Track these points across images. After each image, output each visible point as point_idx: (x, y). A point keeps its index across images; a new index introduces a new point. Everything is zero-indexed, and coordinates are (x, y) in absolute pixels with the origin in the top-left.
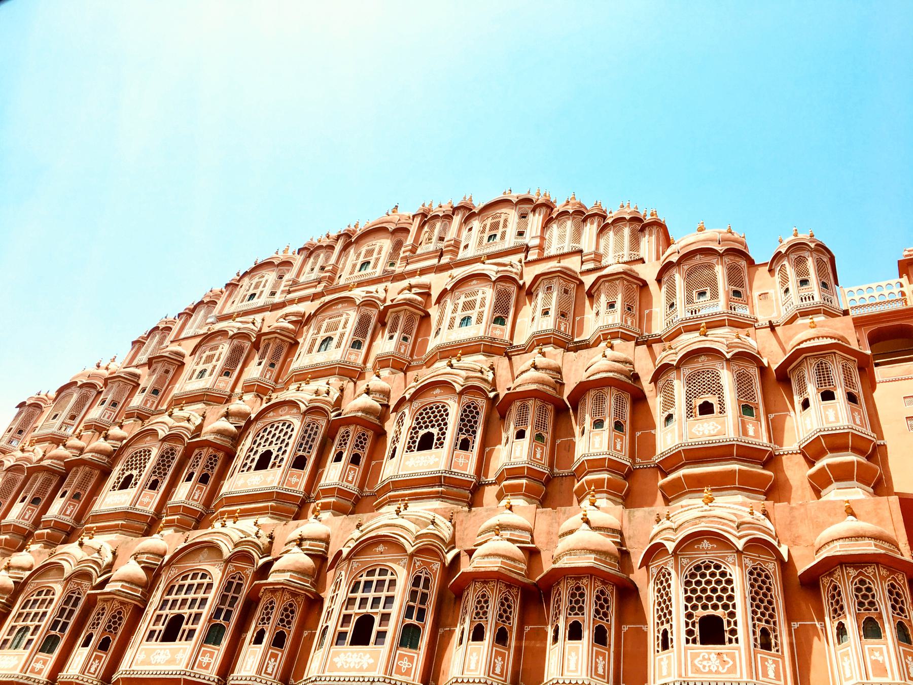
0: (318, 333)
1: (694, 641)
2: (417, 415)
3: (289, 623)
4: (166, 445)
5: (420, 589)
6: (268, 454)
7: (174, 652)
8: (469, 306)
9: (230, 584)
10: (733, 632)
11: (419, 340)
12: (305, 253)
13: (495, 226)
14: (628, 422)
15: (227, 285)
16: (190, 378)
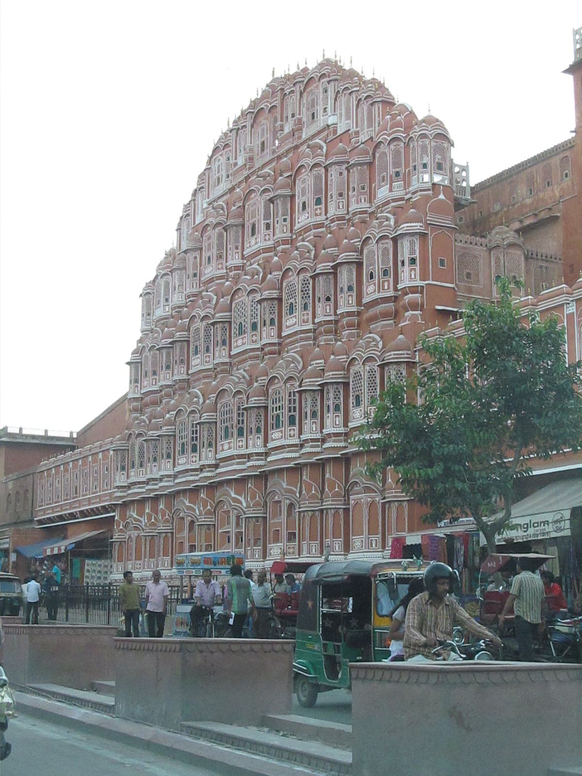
1: (354, 407)
3: (260, 421)
4: (204, 323)
5: (292, 397)
7: (229, 443)
10: (362, 401)
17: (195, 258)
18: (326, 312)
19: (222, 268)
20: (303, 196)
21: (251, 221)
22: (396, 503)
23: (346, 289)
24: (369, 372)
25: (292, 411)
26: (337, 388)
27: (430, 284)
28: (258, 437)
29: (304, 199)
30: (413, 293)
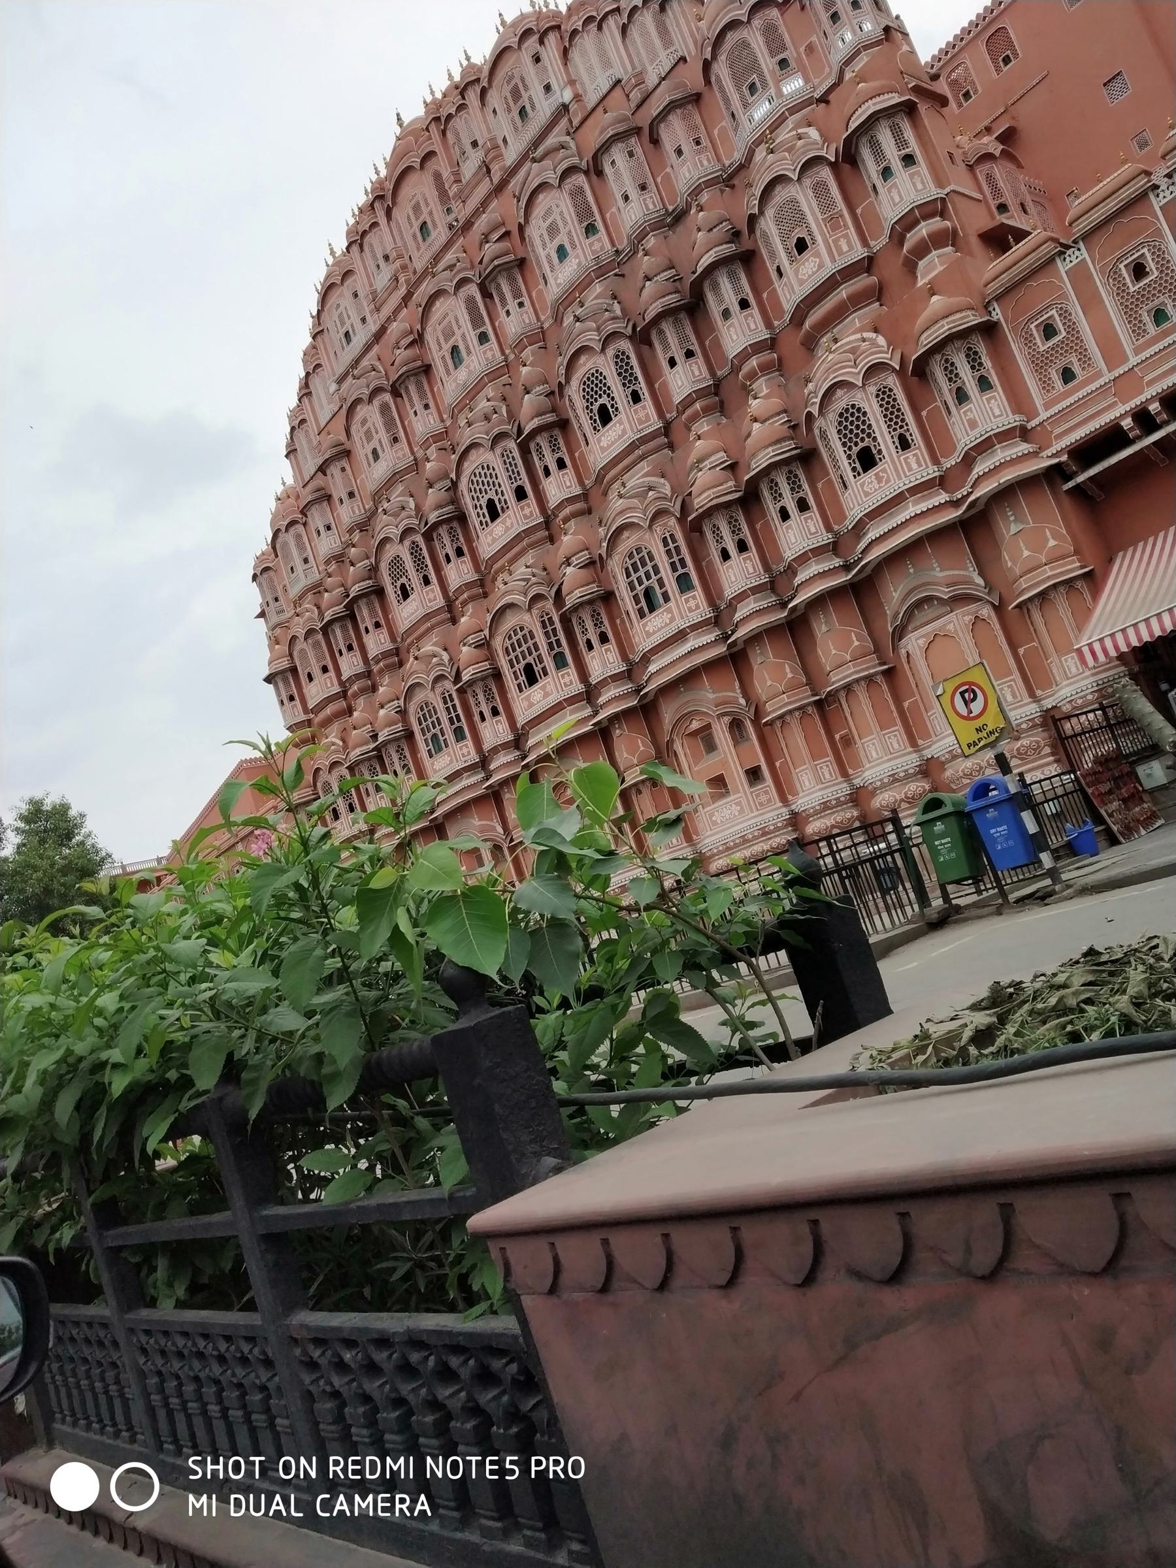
0: (441, 348)
1: (859, 474)
2: (582, 393)
3: (602, 623)
4: (407, 543)
5: (671, 546)
6: (491, 503)
7: (543, 688)
8: (553, 231)
9: (543, 622)
10: (880, 452)
11: (534, 294)
12: (355, 248)
13: (516, 94)
14: (751, 295)
15: (314, 338)
16: (369, 465)
17: (343, 470)
18: (694, 376)
19: (404, 455)
20: (552, 238)
21: (447, 347)
22: (1062, 589)
23: (735, 307)
24: (877, 396)
25: (679, 567)
26: (790, 472)
27: (954, 191)
28: (606, 651)
29: (562, 239)
30: (926, 217)
